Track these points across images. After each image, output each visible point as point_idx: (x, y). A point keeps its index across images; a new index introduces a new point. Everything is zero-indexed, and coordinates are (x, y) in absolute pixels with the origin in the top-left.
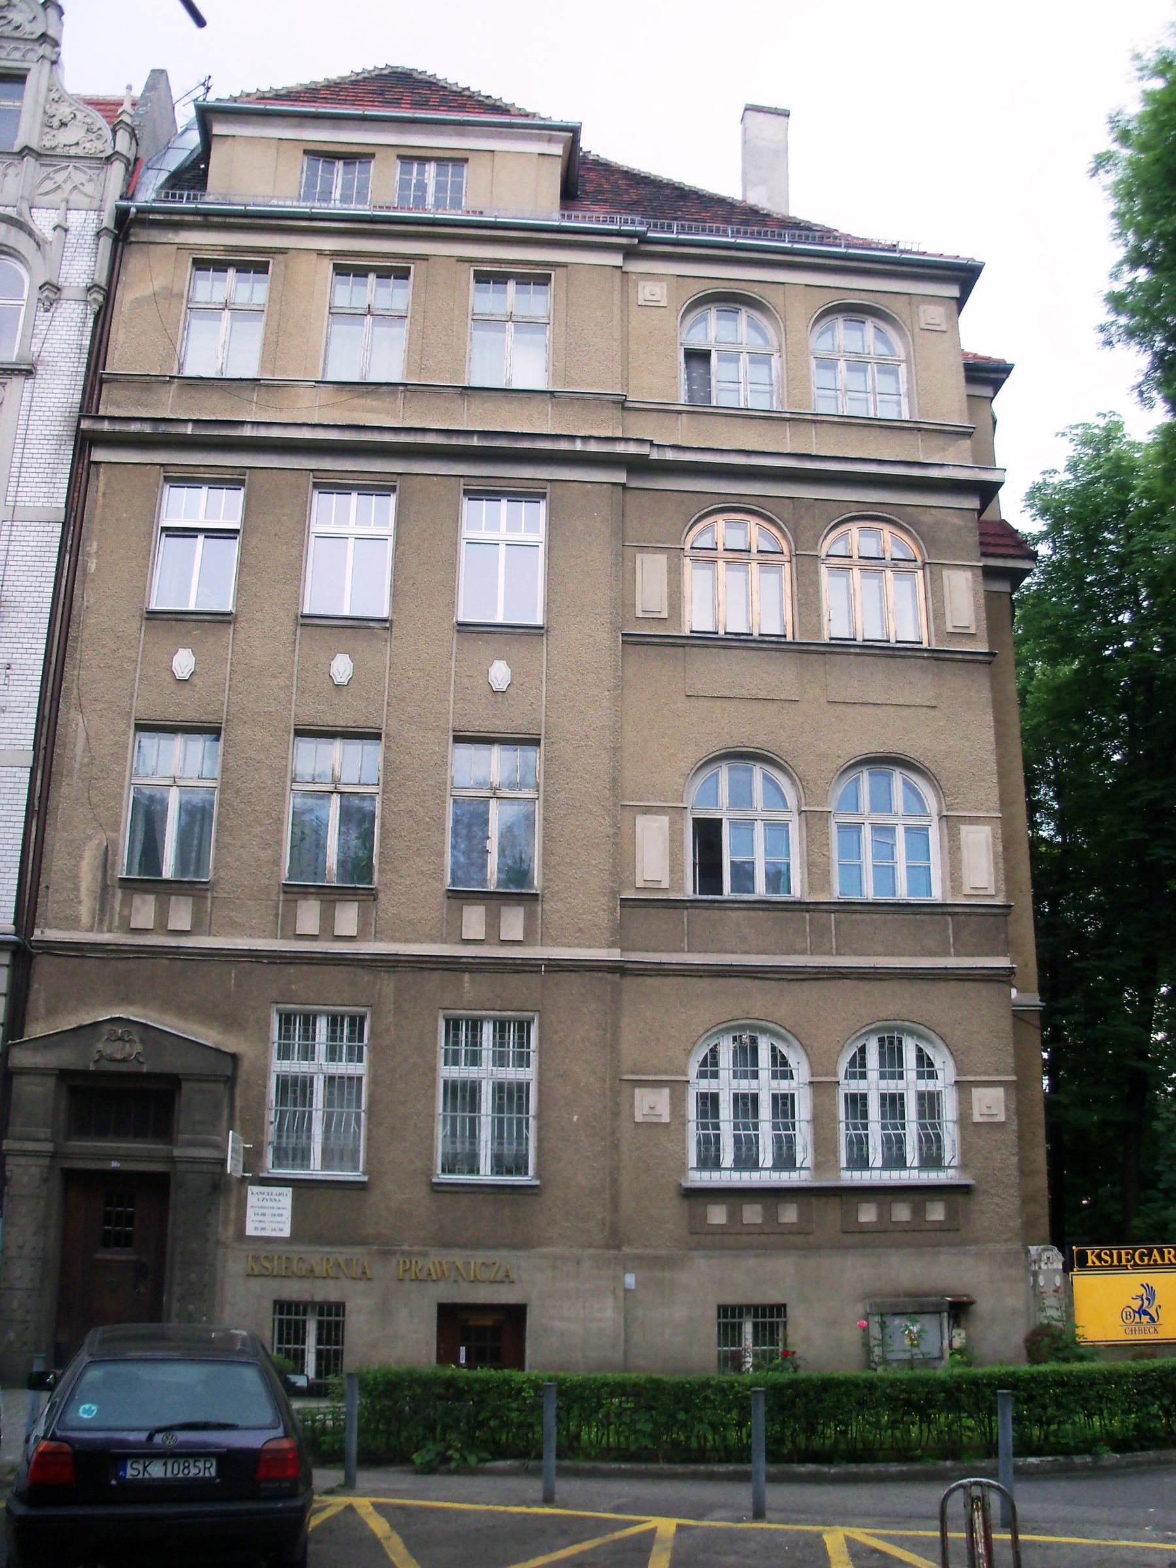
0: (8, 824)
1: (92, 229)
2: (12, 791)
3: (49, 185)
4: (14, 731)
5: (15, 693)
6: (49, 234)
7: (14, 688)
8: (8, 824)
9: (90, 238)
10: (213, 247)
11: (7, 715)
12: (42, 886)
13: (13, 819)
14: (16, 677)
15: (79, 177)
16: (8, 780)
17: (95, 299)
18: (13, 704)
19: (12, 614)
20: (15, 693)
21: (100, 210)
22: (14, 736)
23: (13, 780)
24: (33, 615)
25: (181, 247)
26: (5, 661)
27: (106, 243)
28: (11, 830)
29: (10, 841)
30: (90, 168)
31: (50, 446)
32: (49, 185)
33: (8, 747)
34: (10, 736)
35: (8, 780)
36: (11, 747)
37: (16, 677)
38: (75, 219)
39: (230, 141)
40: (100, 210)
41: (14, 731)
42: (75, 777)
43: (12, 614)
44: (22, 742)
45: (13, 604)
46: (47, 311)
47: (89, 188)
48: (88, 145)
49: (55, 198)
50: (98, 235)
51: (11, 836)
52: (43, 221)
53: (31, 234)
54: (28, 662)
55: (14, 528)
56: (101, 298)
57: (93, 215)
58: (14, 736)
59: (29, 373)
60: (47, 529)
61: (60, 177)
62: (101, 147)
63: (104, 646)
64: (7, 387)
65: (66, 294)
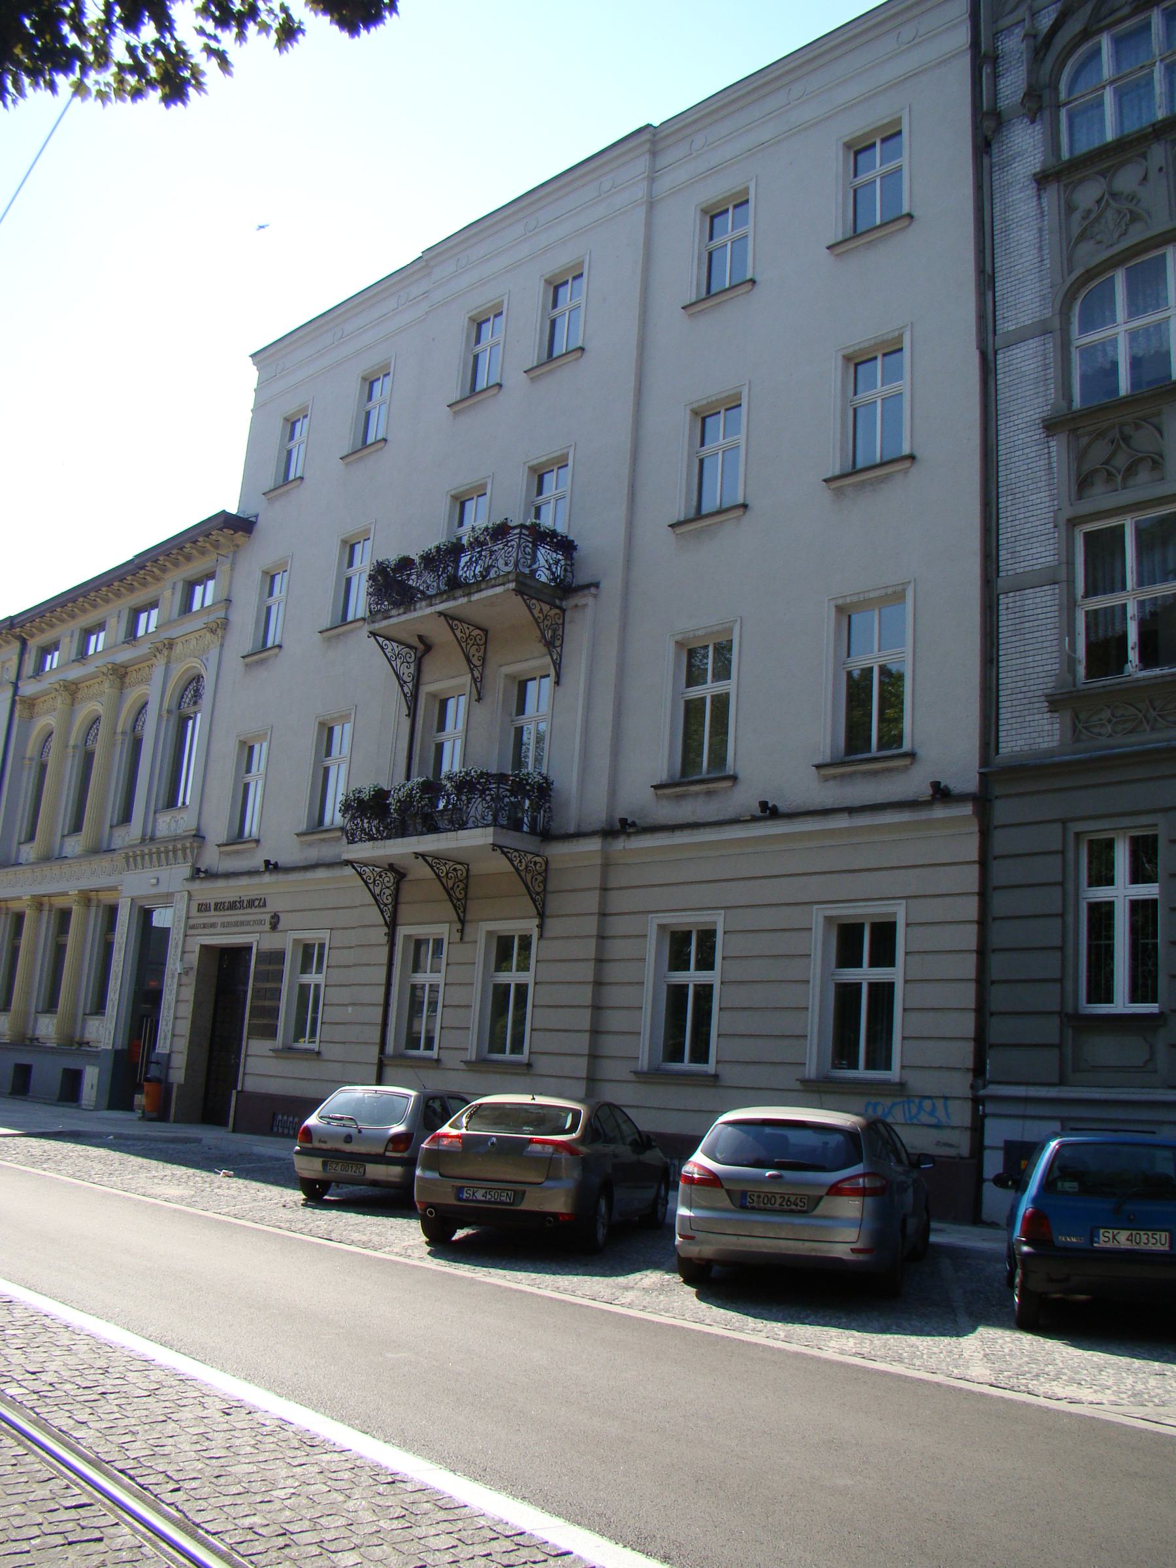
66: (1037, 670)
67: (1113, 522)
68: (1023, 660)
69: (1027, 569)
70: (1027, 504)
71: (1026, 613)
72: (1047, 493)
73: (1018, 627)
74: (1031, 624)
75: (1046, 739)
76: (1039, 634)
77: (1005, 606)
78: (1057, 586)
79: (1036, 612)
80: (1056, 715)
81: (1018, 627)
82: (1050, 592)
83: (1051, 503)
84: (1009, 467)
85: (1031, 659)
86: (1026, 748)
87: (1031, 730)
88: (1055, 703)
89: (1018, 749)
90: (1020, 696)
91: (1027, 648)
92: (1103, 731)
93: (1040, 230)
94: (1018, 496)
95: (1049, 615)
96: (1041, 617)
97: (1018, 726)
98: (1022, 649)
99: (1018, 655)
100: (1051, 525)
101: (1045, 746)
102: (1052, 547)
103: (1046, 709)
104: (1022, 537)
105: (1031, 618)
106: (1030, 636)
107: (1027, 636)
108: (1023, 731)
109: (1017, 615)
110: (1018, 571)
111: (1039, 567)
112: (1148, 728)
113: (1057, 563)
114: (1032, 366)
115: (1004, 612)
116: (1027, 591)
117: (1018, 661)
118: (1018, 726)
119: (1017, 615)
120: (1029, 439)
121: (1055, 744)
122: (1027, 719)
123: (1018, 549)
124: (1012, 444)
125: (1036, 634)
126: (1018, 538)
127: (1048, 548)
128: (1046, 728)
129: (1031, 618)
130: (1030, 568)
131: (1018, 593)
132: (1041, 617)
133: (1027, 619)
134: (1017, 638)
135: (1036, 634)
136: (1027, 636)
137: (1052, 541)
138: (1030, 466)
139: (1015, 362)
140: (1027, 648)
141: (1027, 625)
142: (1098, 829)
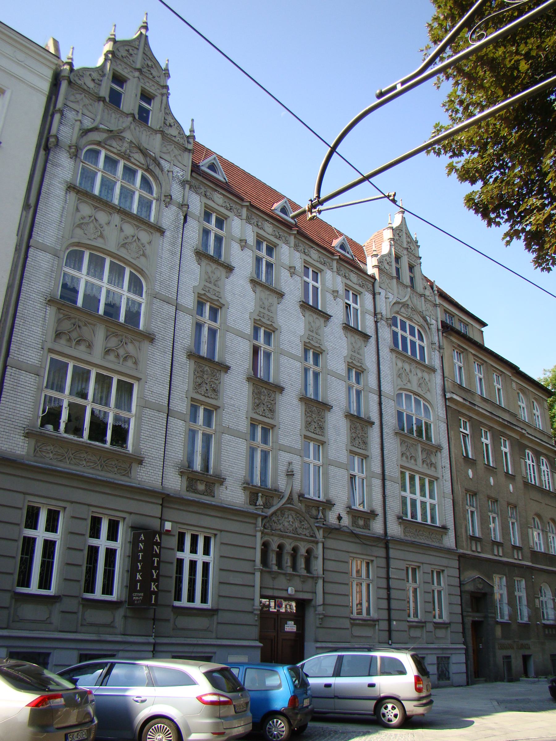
66: (21, 413)
67: (65, 360)
68: (14, 405)
69: (24, 361)
70: (30, 329)
71: (20, 382)
72: (41, 330)
73: (15, 387)
74: (22, 389)
75: (20, 449)
76: (25, 396)
77: (10, 373)
78: (37, 377)
79: (25, 384)
80: (27, 439)
81: (15, 387)
82: (34, 378)
83: (42, 336)
84: (25, 305)
85: (18, 406)
86: (9, 450)
87: (13, 442)
88: (28, 435)
89: (5, 449)
90: (10, 422)
91: (18, 400)
92: (47, 455)
93: (64, 208)
94: (26, 322)
95: (31, 389)
96: (27, 387)
97: (6, 437)
98: (15, 399)
99: (13, 401)
100: (40, 346)
101: (19, 452)
102: (39, 357)
103: (22, 435)
104: (24, 344)
105: (22, 386)
106: (20, 394)
107: (18, 394)
108: (8, 440)
109: (16, 381)
110: (20, 359)
111: (30, 363)
112: (68, 462)
113: (39, 366)
114: (46, 266)
115: (9, 376)
116: (22, 372)
117: (12, 404)
118: (6, 437)
119: (16, 381)
120: (37, 299)
121: (24, 453)
122: (12, 435)
123: (22, 348)
124: (29, 296)
125: (23, 395)
126: (23, 343)
127: (37, 356)
128: (21, 444)
129: (22, 386)
130: (26, 361)
131: (18, 370)
132: (27, 387)
133: (20, 385)
134: (14, 392)
135: (23, 395)
136: (18, 394)
137: (39, 354)
138: (36, 312)
139: (38, 258)
140: (18, 400)
141: (19, 388)
142: (36, 501)
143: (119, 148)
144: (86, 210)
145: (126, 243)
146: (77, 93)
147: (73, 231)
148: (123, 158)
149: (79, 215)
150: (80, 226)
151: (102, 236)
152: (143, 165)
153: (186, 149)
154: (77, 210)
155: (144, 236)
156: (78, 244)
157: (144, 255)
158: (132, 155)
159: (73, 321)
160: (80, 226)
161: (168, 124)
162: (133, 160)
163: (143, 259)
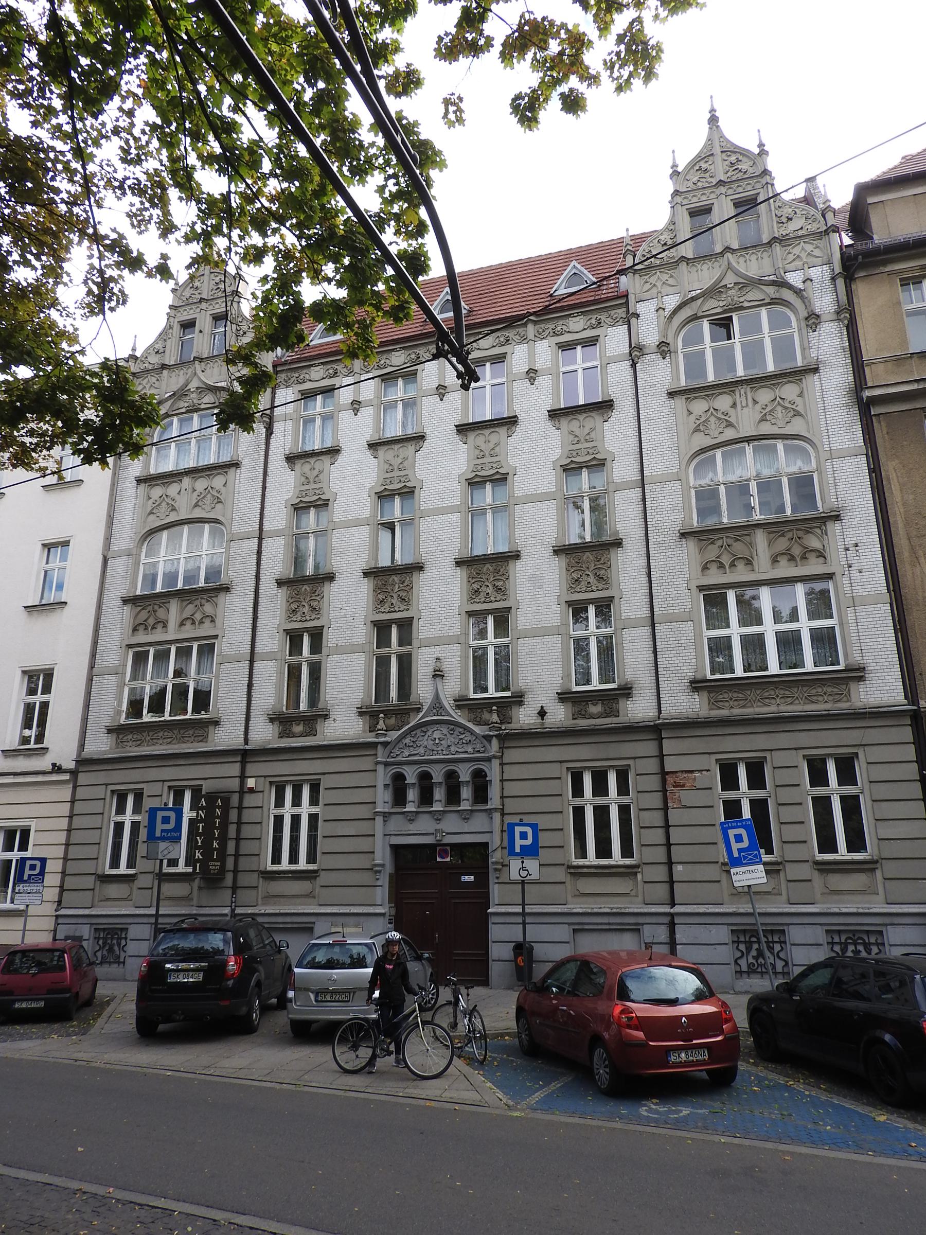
0: (885, 639)
1: (827, 276)
2: (881, 619)
3: (791, 257)
4: (871, 583)
5: (865, 560)
6: (801, 286)
7: (864, 557)
8: (885, 639)
9: (828, 282)
10: (912, 269)
11: (864, 574)
12: (917, 674)
13: (886, 635)
14: (863, 551)
15: (809, 248)
16: (877, 612)
17: (845, 317)
18: (866, 567)
19: (849, 514)
20: (865, 560)
21: (829, 263)
22: (872, 586)
23: (880, 612)
24: (863, 512)
25: (890, 273)
26: (853, 542)
27: (840, 282)
28: (888, 642)
29: (889, 649)
30: (814, 240)
31: (844, 411)
32: (791, 257)
33: (870, 593)
34: (869, 586)
35: (877, 612)
36: (873, 593)
37: (863, 551)
38: (814, 273)
39: (881, 205)
40: (829, 263)
41: (871, 583)
42: (921, 605)
43: (849, 514)
44: (879, 589)
45: (848, 508)
46: (815, 331)
47: (817, 252)
48: (809, 227)
49: (798, 263)
50: (833, 279)
51: (888, 646)
52: (795, 279)
53: (790, 287)
54: (868, 540)
55: (834, 463)
56: (848, 315)
57: (825, 267)
58: (872, 586)
59: (816, 370)
60: (856, 460)
61: (797, 251)
62: (818, 226)
63: (917, 524)
64: (804, 380)
65: (823, 318)
143: (721, 304)
144: (699, 406)
145: (765, 415)
146: (650, 277)
147: (689, 441)
148: (731, 310)
149: (692, 418)
150: (697, 430)
151: (730, 425)
152: (764, 299)
153: (826, 232)
154: (690, 413)
155: (789, 391)
156: (703, 451)
157: (797, 414)
158: (742, 299)
159: (719, 543)
160: (697, 430)
161: (784, 220)
162: (746, 304)
163: (798, 421)
